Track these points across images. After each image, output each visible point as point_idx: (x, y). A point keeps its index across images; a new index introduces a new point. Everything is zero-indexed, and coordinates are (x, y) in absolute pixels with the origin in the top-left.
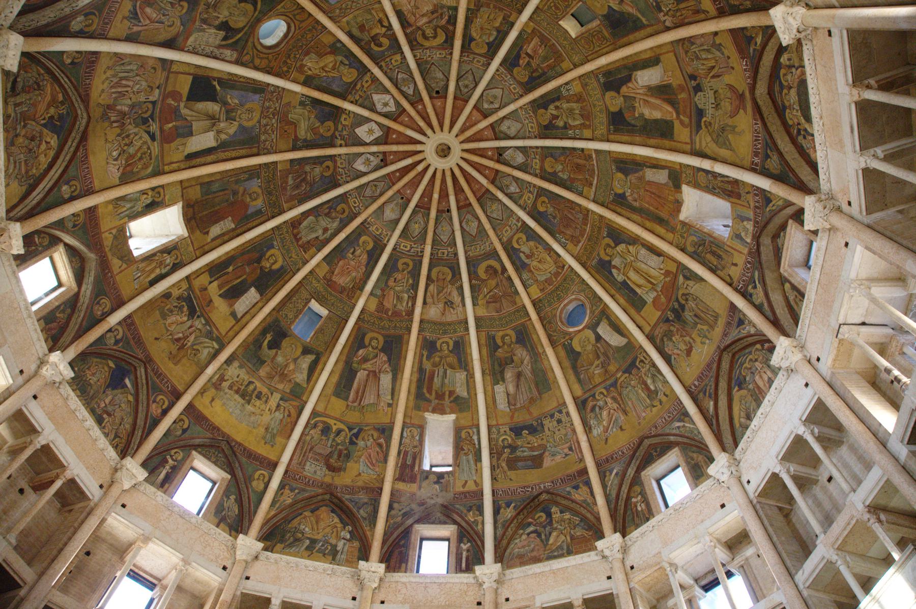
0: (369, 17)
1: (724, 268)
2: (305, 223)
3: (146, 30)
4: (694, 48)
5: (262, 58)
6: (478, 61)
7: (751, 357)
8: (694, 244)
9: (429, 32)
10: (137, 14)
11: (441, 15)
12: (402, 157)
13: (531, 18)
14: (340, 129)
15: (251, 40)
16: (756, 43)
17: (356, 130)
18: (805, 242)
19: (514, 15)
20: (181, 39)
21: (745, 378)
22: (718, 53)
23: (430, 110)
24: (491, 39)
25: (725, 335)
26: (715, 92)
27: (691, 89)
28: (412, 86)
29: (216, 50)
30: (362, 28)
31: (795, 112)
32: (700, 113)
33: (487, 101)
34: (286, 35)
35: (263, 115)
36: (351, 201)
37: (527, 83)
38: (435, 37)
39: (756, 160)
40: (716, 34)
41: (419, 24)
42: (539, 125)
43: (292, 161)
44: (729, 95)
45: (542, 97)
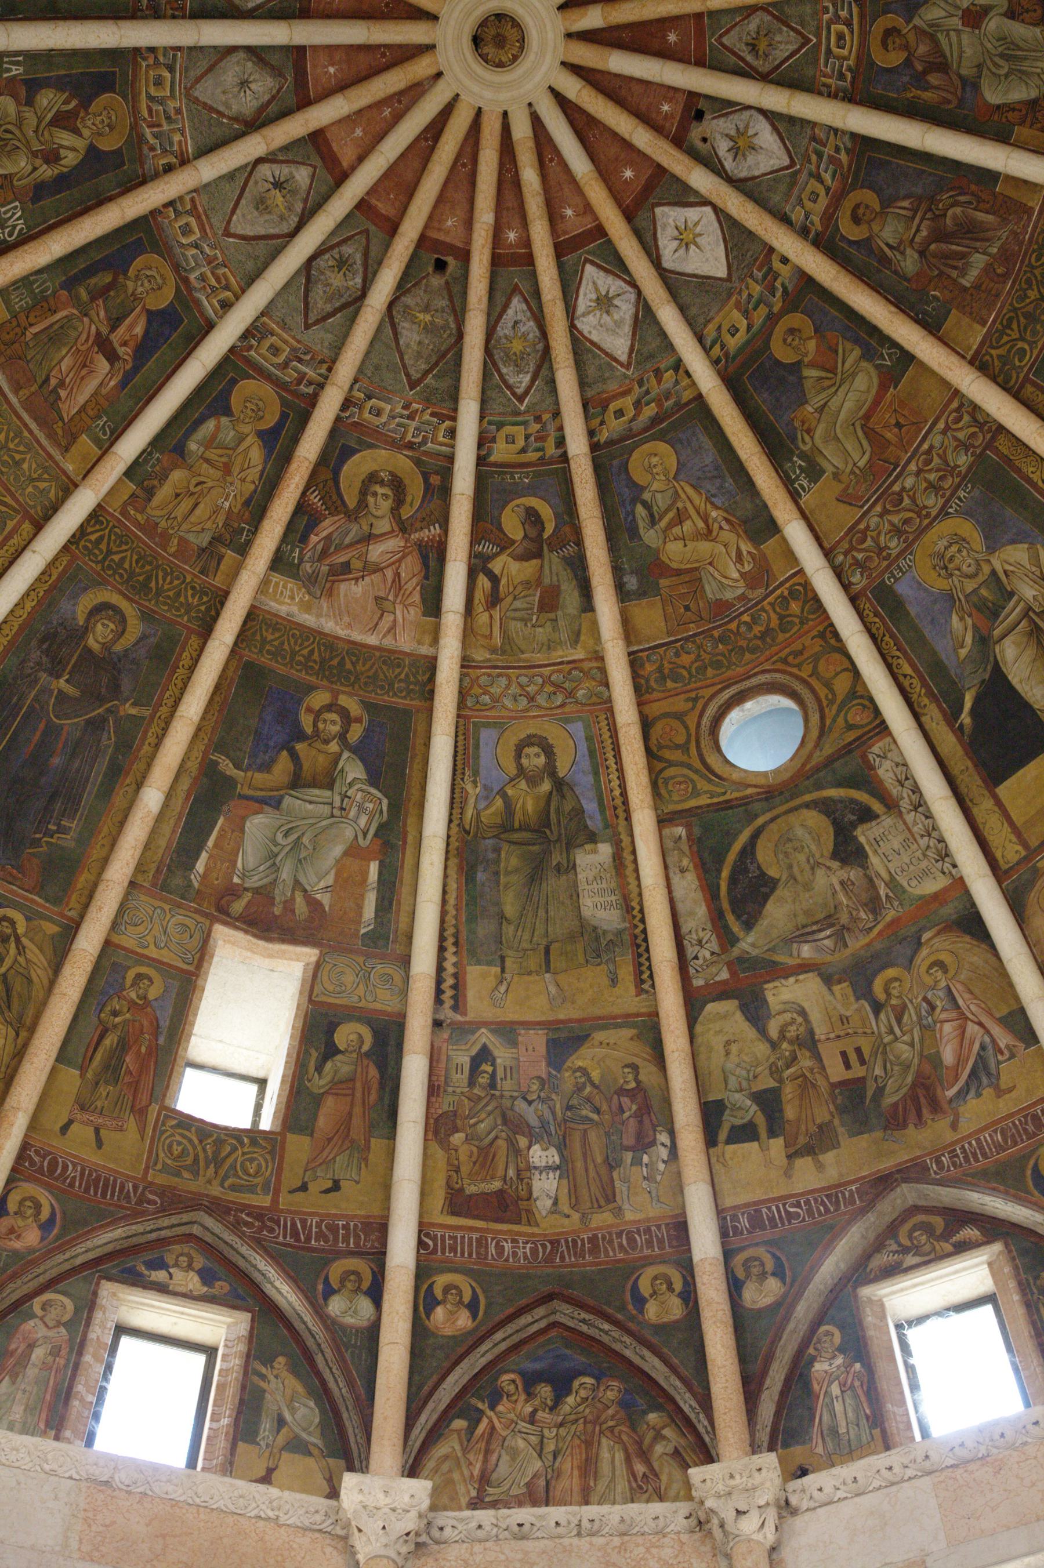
0: (515, 626)
2: (1019, 93)
3: (990, 1014)
5: (828, 685)
6: (275, 350)
9: (381, 503)
10: (973, 1073)
11: (324, 554)
12: (637, 89)
13: (68, 488)
14: (762, 311)
15: (818, 757)
17: (722, 272)
19: (114, 508)
20: (949, 911)
23: (485, 217)
24: (210, 425)
28: (504, 329)
29: (905, 804)
30: (549, 602)
33: (293, 192)
34: (739, 699)
35: (927, 520)
36: (849, 52)
37: (137, 249)
38: (372, 478)
41: (394, 544)
42: (131, 97)
43: (932, 326)
45: (101, 201)
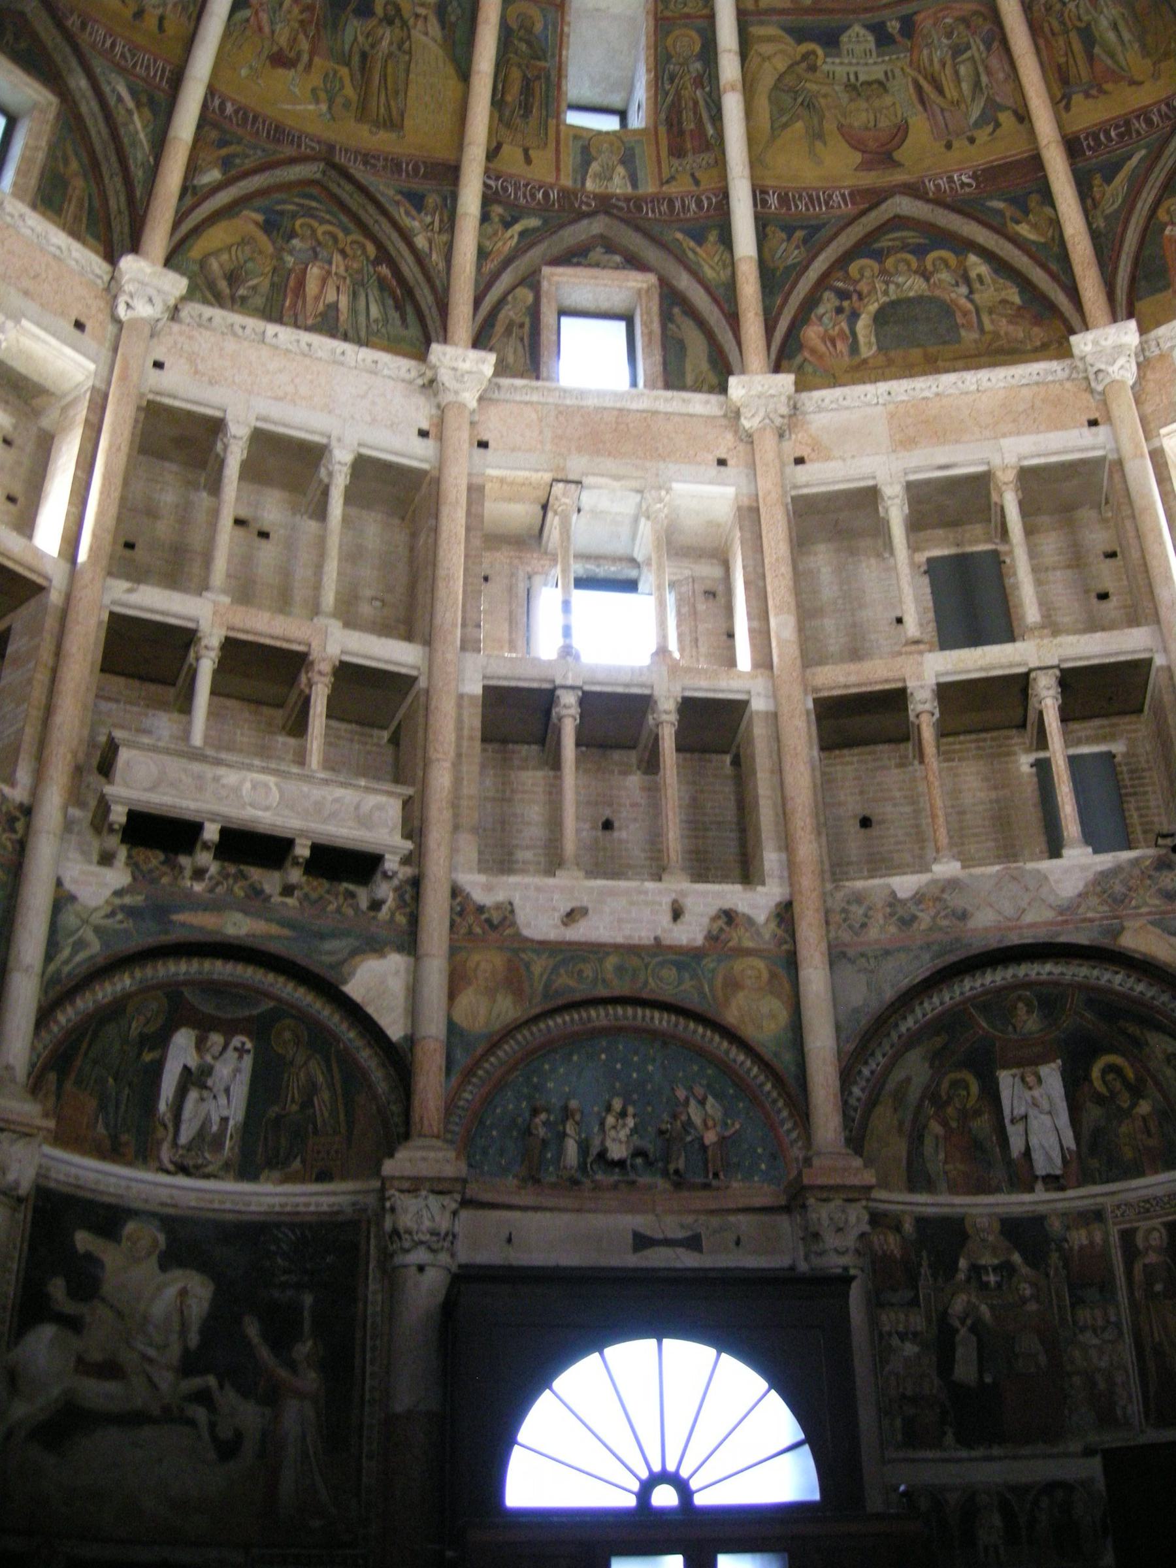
1: (508, 125)
4: (977, 48)
7: (341, 235)
8: (526, 26)
16: (1018, 222)
18: (605, 306)
21: (292, 234)
22: (975, 113)
25: (367, 158)
26: (880, 83)
27: (875, 17)
31: (880, 286)
32: (831, 40)
39: (773, 201)
40: (1023, 116)
44: (884, 123)
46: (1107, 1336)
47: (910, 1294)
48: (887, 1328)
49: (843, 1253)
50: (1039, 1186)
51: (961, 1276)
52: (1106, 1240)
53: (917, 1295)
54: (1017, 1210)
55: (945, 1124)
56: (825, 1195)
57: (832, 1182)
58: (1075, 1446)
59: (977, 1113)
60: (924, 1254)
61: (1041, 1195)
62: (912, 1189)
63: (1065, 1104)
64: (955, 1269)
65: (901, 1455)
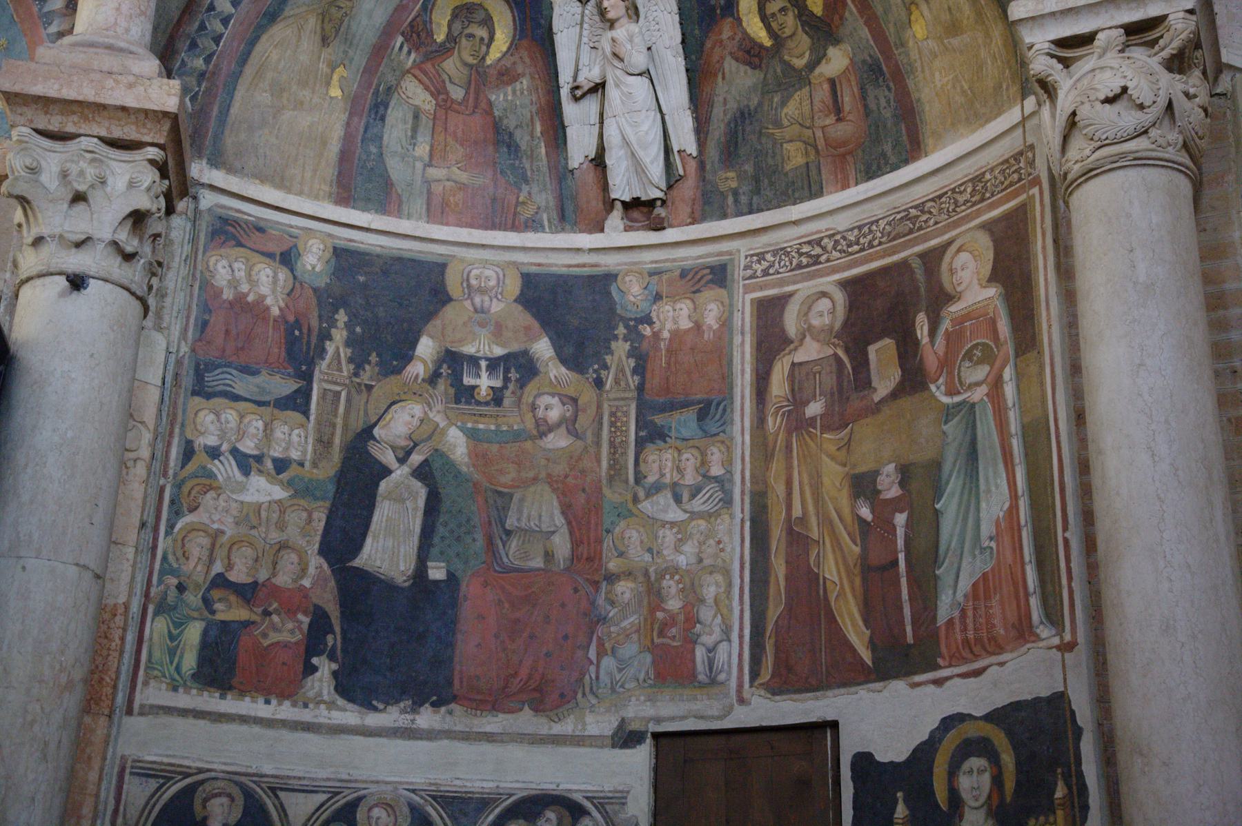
46: (698, 504)
47: (285, 386)
48: (212, 441)
49: (78, 245)
50: (615, 219)
51: (417, 369)
52: (726, 324)
53: (305, 393)
54: (560, 263)
55: (438, 92)
56: (55, 123)
57: (69, 93)
58: (600, 723)
59: (506, 76)
60: (342, 317)
61: (616, 233)
62: (344, 197)
63: (681, 61)
64: (405, 354)
65: (183, 700)
